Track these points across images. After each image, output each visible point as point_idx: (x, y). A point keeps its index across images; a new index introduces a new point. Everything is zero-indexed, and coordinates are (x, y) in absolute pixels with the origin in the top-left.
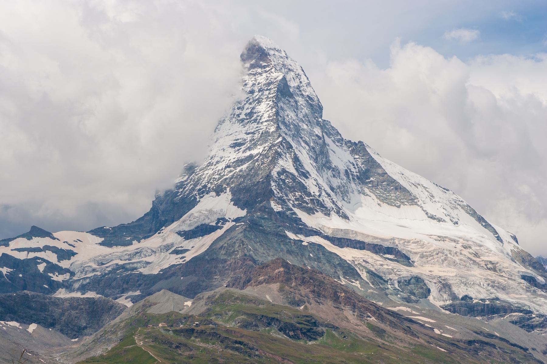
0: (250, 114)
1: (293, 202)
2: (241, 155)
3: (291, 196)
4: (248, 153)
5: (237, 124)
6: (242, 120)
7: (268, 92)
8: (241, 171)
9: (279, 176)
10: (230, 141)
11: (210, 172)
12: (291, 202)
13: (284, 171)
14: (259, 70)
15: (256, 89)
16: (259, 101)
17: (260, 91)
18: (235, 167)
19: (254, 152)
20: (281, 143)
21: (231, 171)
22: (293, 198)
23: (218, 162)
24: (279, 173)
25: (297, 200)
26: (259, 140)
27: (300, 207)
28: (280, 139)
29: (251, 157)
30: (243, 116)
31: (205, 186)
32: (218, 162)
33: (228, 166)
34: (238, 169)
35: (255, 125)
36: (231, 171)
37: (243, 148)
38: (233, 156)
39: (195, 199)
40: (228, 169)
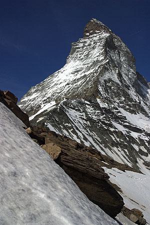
0: (87, 55)
1: (118, 103)
2: (79, 76)
3: (115, 99)
4: (83, 75)
5: (78, 61)
6: (82, 59)
7: (99, 44)
8: (76, 85)
9: (106, 83)
10: (72, 70)
11: (55, 89)
12: (117, 104)
13: (110, 80)
14: (95, 35)
15: (92, 43)
16: (94, 48)
17: (94, 44)
18: (72, 84)
19: (87, 73)
20: (108, 62)
21: (69, 87)
22: (118, 101)
23: (61, 83)
24: (105, 81)
25: (121, 103)
26: (91, 66)
27: (123, 107)
28: (108, 60)
29: (85, 76)
30: (83, 57)
31: (49, 98)
32: (61, 83)
33: (68, 84)
34: (75, 84)
35: (91, 60)
36: (69, 87)
37: (80, 73)
38: (72, 77)
39: (40, 106)
40: (67, 86)
